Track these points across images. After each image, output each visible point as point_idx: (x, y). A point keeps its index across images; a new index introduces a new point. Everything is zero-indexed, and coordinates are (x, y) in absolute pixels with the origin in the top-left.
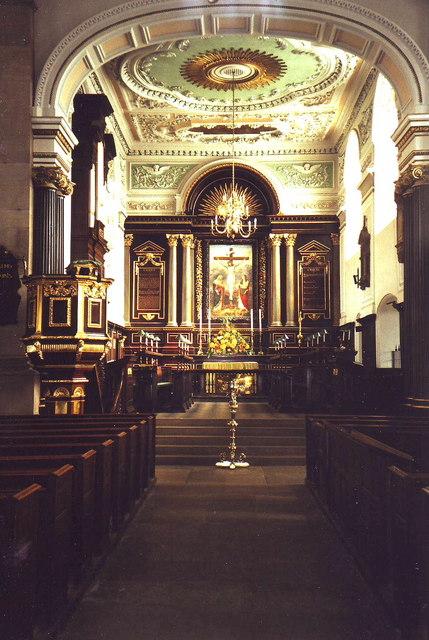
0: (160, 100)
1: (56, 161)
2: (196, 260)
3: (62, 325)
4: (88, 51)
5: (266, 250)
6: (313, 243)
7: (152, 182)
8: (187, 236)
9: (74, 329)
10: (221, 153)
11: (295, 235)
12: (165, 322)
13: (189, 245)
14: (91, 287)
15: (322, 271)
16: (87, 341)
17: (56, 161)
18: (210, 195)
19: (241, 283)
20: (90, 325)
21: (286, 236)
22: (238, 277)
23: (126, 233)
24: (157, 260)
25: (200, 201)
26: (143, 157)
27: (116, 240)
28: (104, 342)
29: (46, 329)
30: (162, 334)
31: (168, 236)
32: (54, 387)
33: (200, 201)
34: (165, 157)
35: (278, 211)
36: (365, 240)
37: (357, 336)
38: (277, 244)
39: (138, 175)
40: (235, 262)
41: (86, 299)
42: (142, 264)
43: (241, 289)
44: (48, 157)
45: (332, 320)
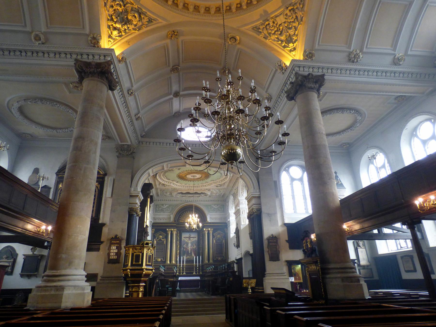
0: (168, 184)
1: (137, 206)
5: (202, 235)
7: (162, 210)
8: (174, 229)
10: (187, 200)
11: (213, 229)
12: (165, 262)
13: (175, 233)
17: (137, 206)
18: (183, 215)
19: (193, 246)
21: (209, 229)
22: (192, 243)
24: (163, 239)
25: (179, 217)
26: (159, 202)
31: (167, 229)
32: (133, 287)
33: (179, 217)
34: (167, 202)
35: (206, 220)
36: (237, 232)
37: (235, 266)
38: (206, 232)
40: (191, 239)
42: (158, 240)
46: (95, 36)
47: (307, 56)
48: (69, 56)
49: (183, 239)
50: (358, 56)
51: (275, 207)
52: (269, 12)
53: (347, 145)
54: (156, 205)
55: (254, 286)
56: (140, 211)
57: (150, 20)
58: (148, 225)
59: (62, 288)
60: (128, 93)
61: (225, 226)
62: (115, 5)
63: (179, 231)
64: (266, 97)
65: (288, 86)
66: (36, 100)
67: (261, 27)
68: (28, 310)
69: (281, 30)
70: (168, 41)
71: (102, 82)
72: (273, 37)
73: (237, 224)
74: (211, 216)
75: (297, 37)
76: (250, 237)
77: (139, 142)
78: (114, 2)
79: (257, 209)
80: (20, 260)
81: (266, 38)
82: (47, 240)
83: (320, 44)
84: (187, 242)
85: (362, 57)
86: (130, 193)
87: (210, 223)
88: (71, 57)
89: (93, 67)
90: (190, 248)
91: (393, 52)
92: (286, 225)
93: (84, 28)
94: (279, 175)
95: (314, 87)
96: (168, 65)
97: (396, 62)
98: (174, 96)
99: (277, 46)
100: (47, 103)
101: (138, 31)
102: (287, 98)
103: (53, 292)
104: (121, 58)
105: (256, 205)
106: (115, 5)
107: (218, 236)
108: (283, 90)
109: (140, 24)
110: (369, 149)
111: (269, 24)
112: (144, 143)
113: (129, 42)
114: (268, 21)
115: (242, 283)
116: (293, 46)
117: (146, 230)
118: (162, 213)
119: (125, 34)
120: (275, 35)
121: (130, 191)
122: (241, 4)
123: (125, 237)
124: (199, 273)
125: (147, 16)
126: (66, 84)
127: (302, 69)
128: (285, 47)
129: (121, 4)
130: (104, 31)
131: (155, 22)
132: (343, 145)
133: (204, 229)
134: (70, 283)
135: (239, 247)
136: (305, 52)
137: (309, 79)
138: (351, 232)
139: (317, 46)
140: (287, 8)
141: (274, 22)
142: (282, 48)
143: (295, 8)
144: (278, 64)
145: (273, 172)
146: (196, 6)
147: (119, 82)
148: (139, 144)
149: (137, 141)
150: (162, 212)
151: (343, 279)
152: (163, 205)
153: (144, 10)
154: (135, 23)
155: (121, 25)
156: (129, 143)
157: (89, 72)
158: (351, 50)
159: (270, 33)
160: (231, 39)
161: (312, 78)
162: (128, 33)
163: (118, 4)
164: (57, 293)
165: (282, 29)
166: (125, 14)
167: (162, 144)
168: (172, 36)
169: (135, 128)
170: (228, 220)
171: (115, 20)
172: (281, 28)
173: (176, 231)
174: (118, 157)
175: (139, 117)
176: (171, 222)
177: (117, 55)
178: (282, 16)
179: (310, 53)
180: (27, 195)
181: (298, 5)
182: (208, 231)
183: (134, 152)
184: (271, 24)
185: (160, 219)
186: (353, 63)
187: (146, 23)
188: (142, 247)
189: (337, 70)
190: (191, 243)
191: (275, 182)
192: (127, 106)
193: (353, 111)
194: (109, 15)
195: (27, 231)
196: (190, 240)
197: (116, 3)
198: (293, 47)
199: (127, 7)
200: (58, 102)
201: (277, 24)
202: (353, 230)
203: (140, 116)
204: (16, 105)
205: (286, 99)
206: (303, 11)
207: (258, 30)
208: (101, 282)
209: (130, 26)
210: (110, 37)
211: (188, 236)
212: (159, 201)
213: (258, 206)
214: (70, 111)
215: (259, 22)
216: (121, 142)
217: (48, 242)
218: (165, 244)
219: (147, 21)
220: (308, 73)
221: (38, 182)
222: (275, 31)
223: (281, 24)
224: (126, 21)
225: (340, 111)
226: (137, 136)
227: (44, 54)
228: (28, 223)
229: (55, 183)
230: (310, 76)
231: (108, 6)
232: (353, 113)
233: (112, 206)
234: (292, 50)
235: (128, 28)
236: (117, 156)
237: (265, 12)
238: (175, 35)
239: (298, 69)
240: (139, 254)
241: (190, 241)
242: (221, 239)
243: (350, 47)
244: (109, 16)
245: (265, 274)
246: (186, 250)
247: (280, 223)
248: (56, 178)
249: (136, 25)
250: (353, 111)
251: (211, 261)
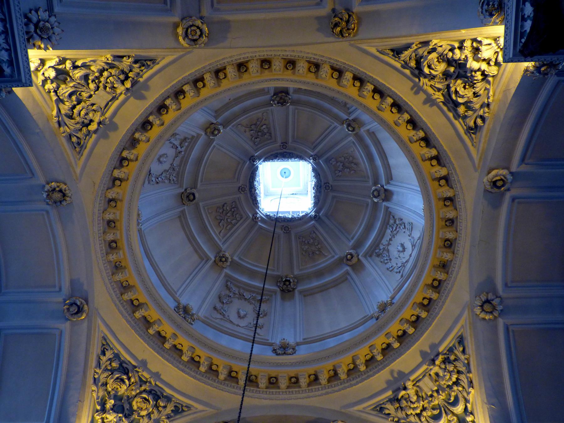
69: (90, 81)
111: (123, 82)
201: (105, 87)
222: (101, 75)
234: (41, 67)
237: (142, 97)
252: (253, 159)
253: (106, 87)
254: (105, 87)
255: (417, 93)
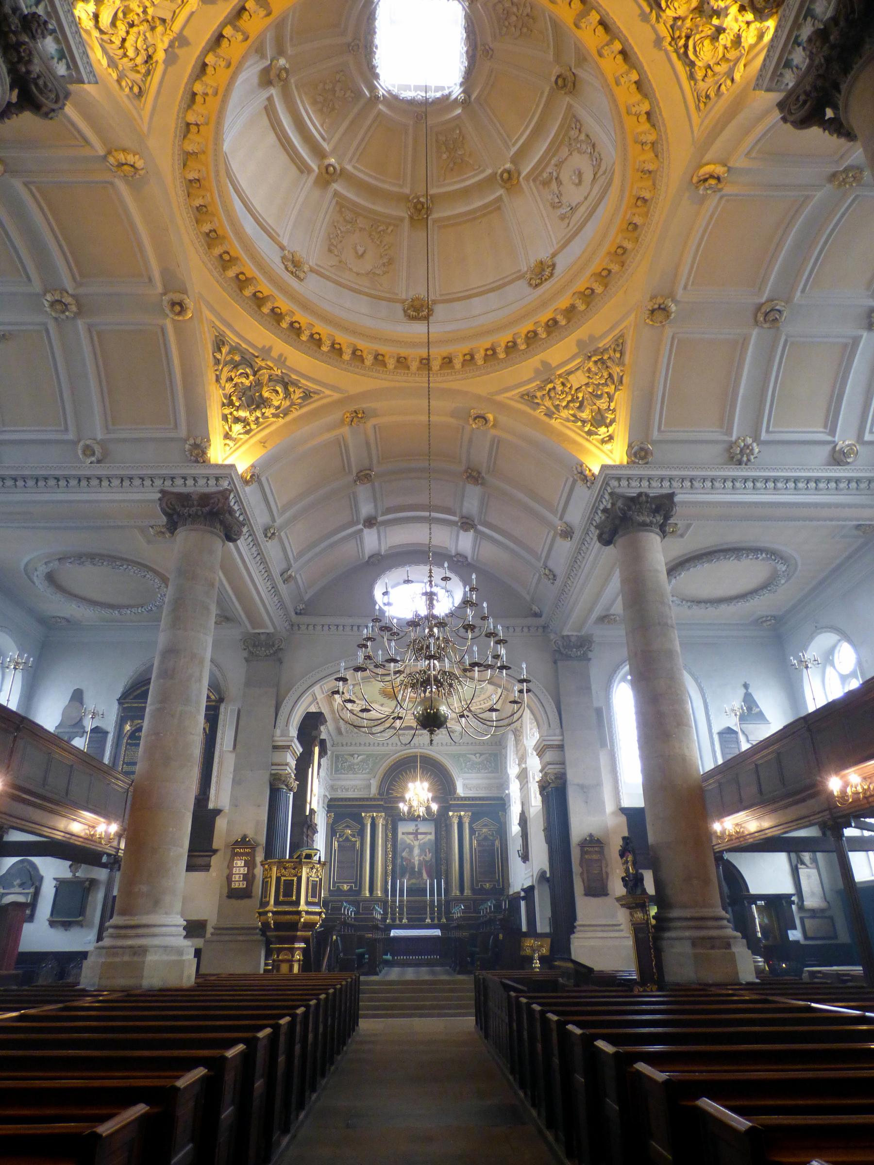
1: (288, 769)
2: (387, 835)
3: (289, 899)
4: (316, 689)
5: (446, 826)
6: (485, 819)
7: (351, 768)
9: (297, 903)
12: (359, 891)
13: (380, 823)
14: (312, 868)
15: (493, 845)
16: (307, 913)
17: (288, 769)
18: (399, 778)
19: (426, 855)
20: (310, 899)
21: (462, 813)
22: (422, 848)
23: (328, 812)
24: (353, 836)
25: (391, 784)
26: (345, 748)
27: (321, 821)
28: (319, 914)
29: (277, 903)
30: (356, 904)
31: (363, 814)
32: (279, 951)
36: (523, 821)
37: (523, 903)
38: (455, 821)
39: (340, 766)
40: (420, 837)
41: (308, 879)
42: (341, 839)
43: (426, 862)
44: (282, 765)
45: (503, 889)
46: (198, 441)
47: (635, 455)
48: (147, 482)
49: (400, 836)
50: (748, 451)
51: (598, 769)
52: (553, 366)
53: (770, 620)
54: (337, 757)
55: (548, 954)
56: (296, 780)
57: (306, 394)
58: (316, 809)
59: (143, 951)
60: (266, 536)
61: (501, 804)
62: (236, 376)
63: (390, 819)
64: (562, 531)
65: (599, 517)
66: (82, 560)
67: (539, 394)
68: (84, 990)
69: (580, 399)
70: (346, 430)
71: (212, 532)
72: (565, 413)
73: (523, 804)
74: (466, 781)
75: (615, 415)
76: (546, 836)
77: (292, 625)
78: (235, 370)
79: (556, 774)
80: (48, 891)
81: (549, 415)
82: (108, 851)
83: (663, 428)
84: (409, 844)
85: (760, 452)
86: (273, 741)
87: (465, 799)
88: (152, 485)
89: (195, 503)
90: (417, 858)
91: (829, 438)
92: (624, 811)
93: (176, 426)
94: (609, 695)
95: (651, 522)
96: (347, 471)
97: (838, 458)
98: (365, 526)
99: (573, 432)
100: (103, 563)
101: (282, 418)
102: (600, 542)
103: (126, 958)
104: (248, 477)
105: (553, 764)
106: (236, 376)
107: (484, 830)
108: (593, 519)
109: (288, 403)
110: (819, 631)
111: (554, 388)
112: (303, 627)
113: (264, 443)
114: (551, 382)
115: (519, 947)
116: (608, 431)
117: (311, 821)
118: (350, 776)
119: (257, 427)
120: (568, 410)
121: (273, 736)
122: (494, 350)
123: (262, 839)
124: (439, 919)
125: (300, 388)
126: (142, 530)
127: (624, 483)
128: (590, 433)
129: (249, 372)
130: (216, 427)
131: (316, 397)
132: (761, 620)
133: (451, 814)
134: (156, 941)
135: (528, 860)
136: (630, 446)
137: (640, 504)
138: (743, 837)
139: (656, 433)
140: (590, 357)
141: (563, 384)
142: (584, 435)
143: (606, 357)
144: (576, 468)
145: (594, 687)
146: (400, 357)
147: (246, 522)
148: (292, 629)
149: (287, 623)
150: (351, 772)
151: (695, 942)
152: (352, 755)
153: (294, 377)
154: (276, 403)
155: (248, 413)
156: (271, 630)
157: (187, 515)
158: (734, 438)
159: (558, 405)
160: (475, 419)
161: (647, 502)
162: (263, 423)
163: (242, 373)
164: (135, 959)
165: (583, 397)
166: (257, 388)
167: (341, 628)
168: (352, 421)
169: (282, 598)
170: (507, 792)
171: (237, 404)
172: (580, 395)
173: (384, 819)
174: (247, 660)
175: (290, 576)
176: (371, 796)
177: (240, 473)
178: (579, 373)
179: (642, 449)
180: (72, 766)
181: (611, 352)
182: (460, 817)
183: (281, 649)
184: (559, 388)
185: (347, 790)
186: (740, 464)
187: (299, 401)
188: (298, 865)
189: (704, 481)
190: (419, 845)
191: (599, 712)
192: (263, 561)
193: (764, 555)
194: (225, 395)
195: (73, 837)
196: (418, 839)
197: (238, 373)
198: (608, 434)
199: (261, 375)
200: (126, 560)
201: (570, 388)
202: (746, 833)
203: (293, 574)
204: (42, 570)
205: (598, 544)
206: (624, 365)
207: (533, 399)
208: (215, 938)
209: (268, 410)
210: (227, 436)
211: (412, 831)
212: (343, 746)
213: (558, 766)
214: (148, 576)
215: (534, 384)
216: (254, 628)
217: (109, 855)
218: (358, 851)
219: (299, 398)
220: (638, 491)
221: (81, 720)
222: (569, 402)
223: (581, 387)
224: (256, 402)
225: (732, 556)
226: (286, 614)
227: (101, 481)
228: (74, 820)
229: (116, 722)
230: (644, 498)
231: (223, 381)
232: (763, 559)
233: (234, 771)
234: (605, 439)
235: (263, 414)
236: (245, 658)
237: (545, 364)
238: (358, 417)
239: (616, 483)
240: (292, 878)
241: (416, 843)
242: (491, 838)
243: (729, 432)
244: (226, 399)
245: (575, 927)
246: (407, 864)
247: (610, 807)
248: (118, 709)
249: (278, 408)
250: (764, 555)
251: (467, 892)
252: (466, 103)
253: (570, 388)
254: (570, 388)
255: (281, 356)
